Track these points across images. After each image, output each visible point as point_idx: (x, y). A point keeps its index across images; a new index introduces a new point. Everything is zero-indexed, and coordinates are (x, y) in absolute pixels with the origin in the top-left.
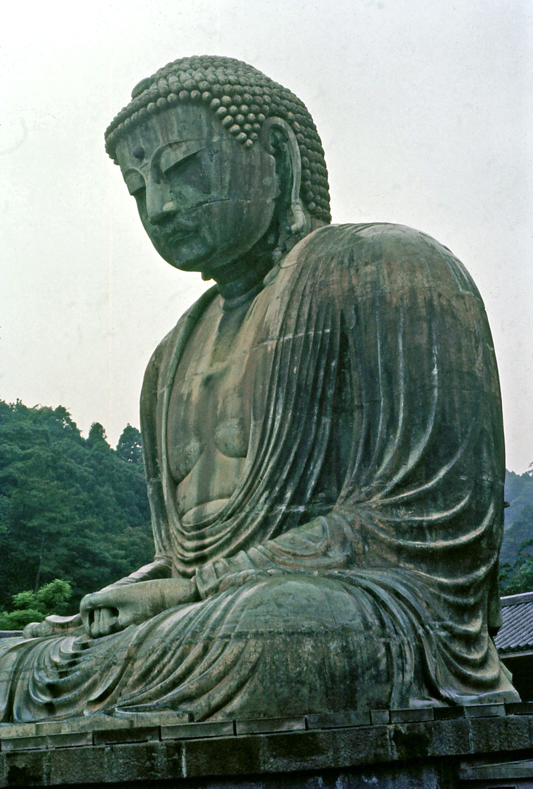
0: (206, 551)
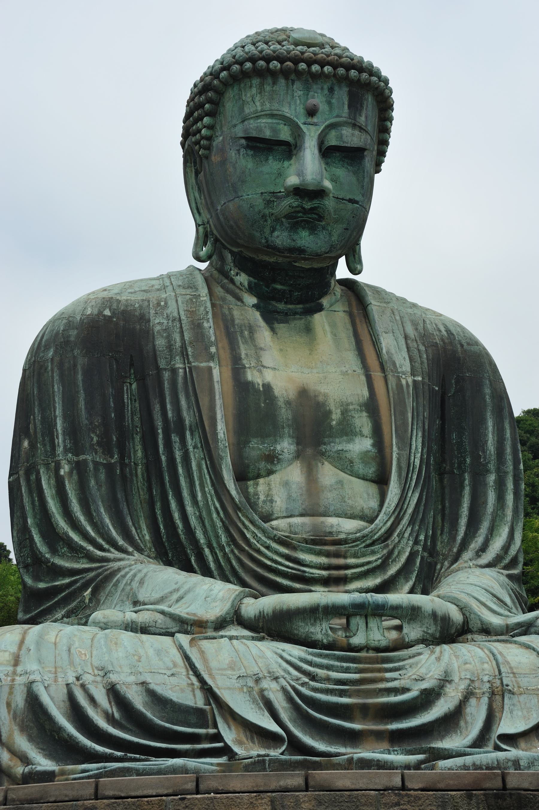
0: (349, 572)
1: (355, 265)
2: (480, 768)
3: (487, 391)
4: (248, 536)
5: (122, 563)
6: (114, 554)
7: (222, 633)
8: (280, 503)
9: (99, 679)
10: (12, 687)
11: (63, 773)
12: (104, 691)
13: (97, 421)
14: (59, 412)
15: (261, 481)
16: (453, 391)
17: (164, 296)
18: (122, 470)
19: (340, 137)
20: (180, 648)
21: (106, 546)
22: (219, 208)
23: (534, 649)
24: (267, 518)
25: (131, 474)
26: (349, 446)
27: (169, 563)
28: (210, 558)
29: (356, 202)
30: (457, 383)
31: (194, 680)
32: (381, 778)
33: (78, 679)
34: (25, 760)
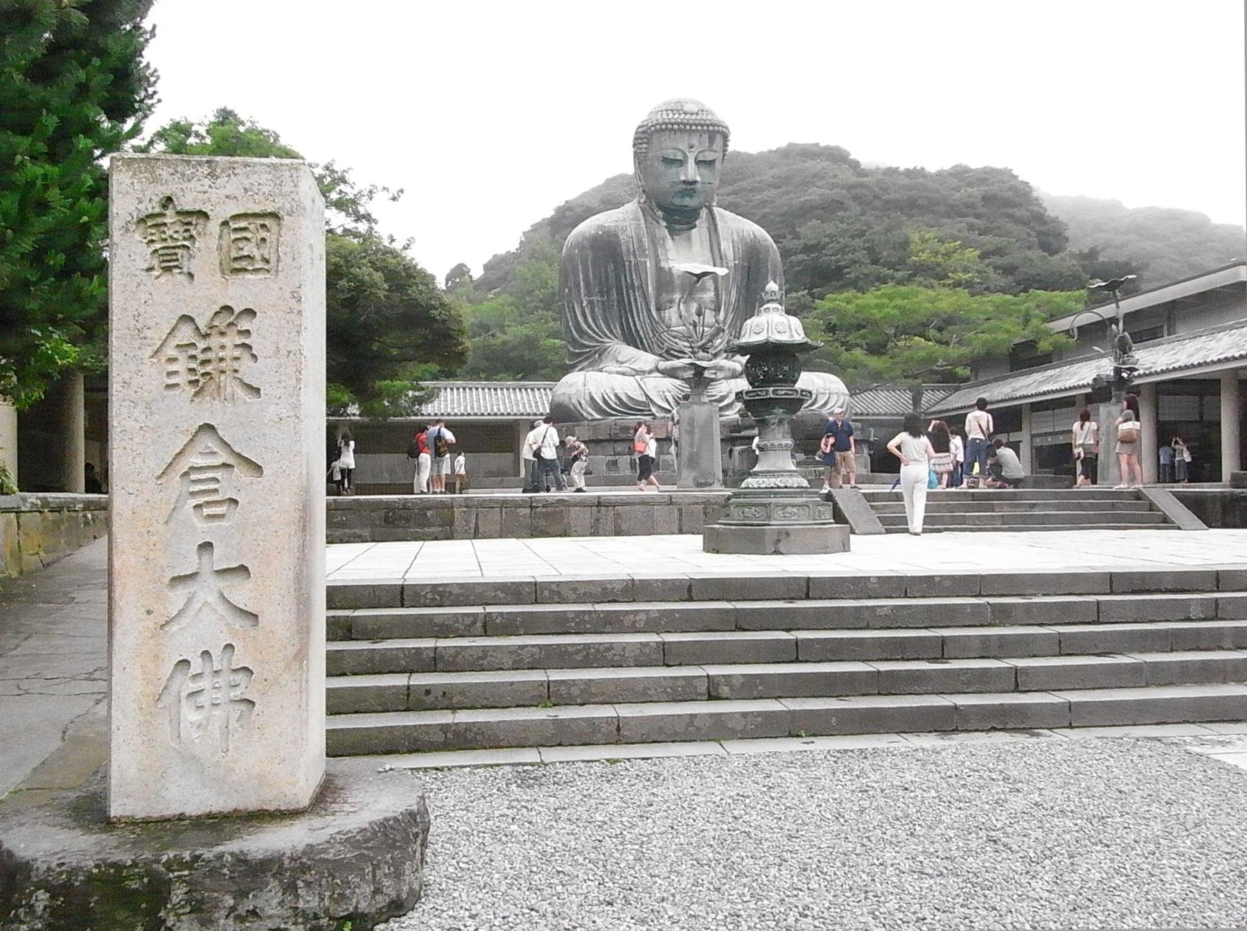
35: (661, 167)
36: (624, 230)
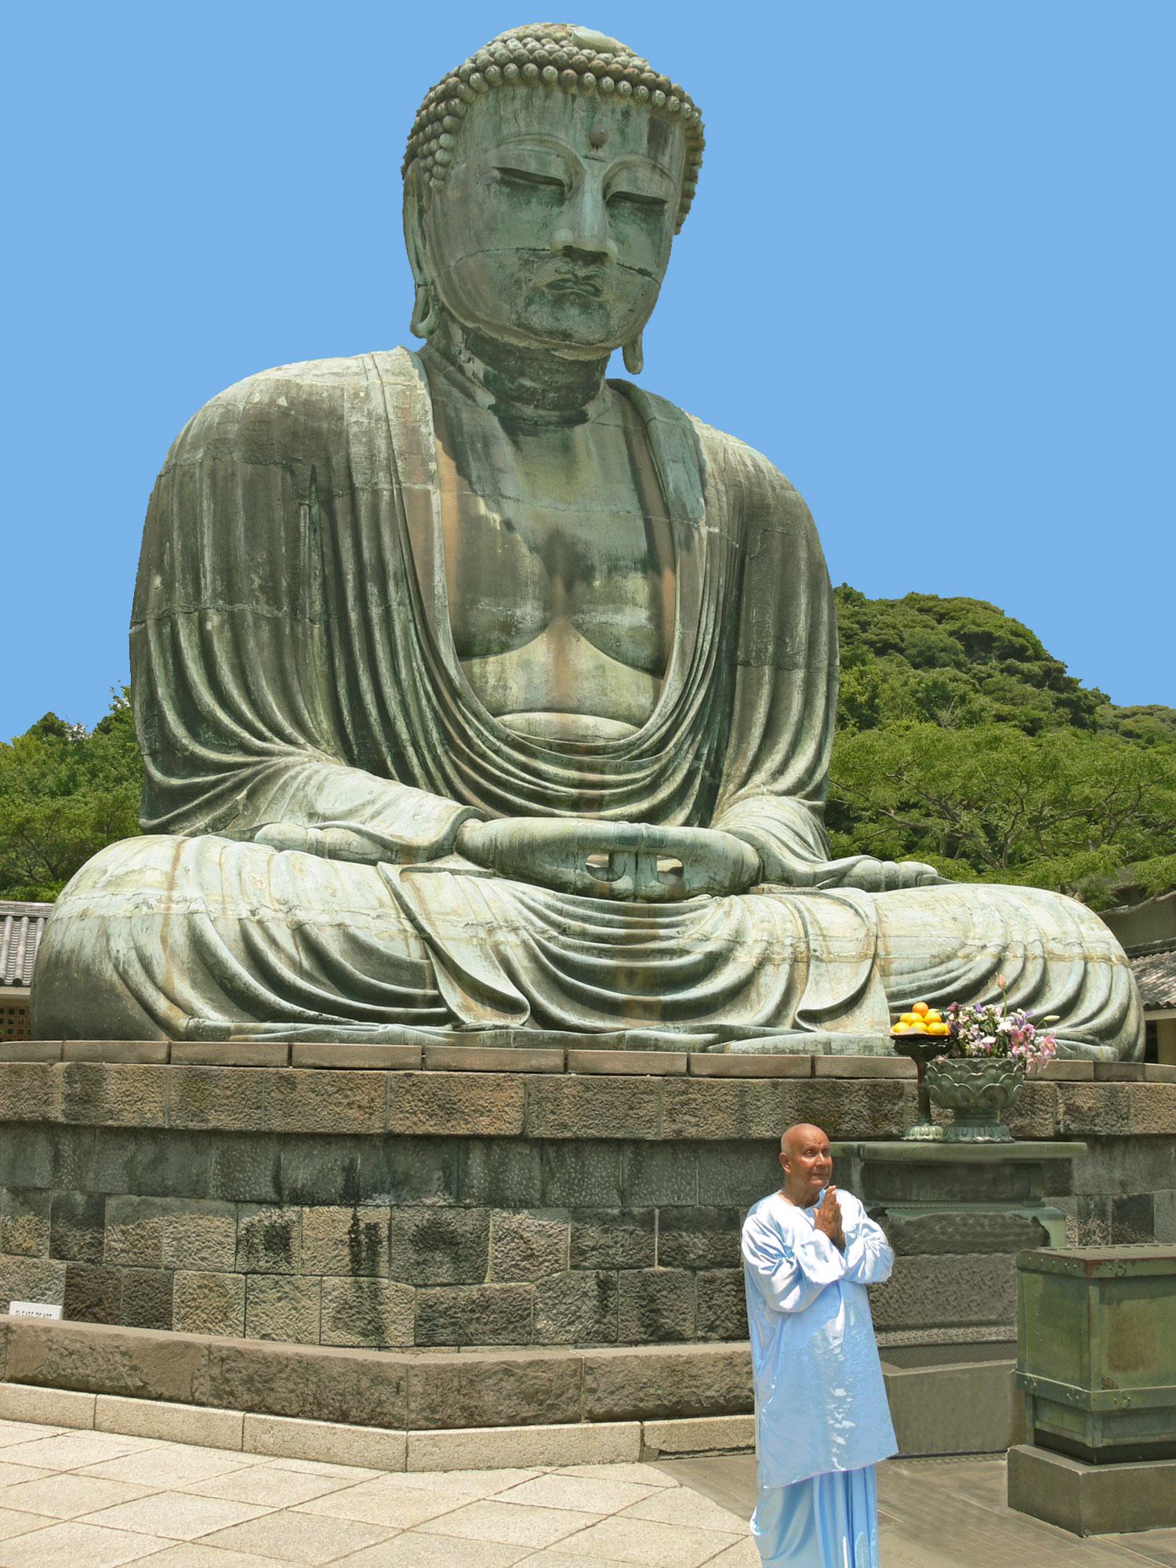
1: (633, 359)
2: (783, 1052)
3: (803, 554)
4: (471, 733)
5: (290, 759)
6: (279, 745)
7: (437, 864)
8: (516, 692)
9: (281, 915)
10: (167, 918)
11: (240, 1031)
12: (288, 932)
13: (261, 556)
14: (207, 540)
15: (491, 659)
16: (757, 550)
17: (364, 383)
18: (292, 629)
19: (634, 181)
20: (388, 882)
21: (268, 734)
22: (453, 263)
23: (851, 906)
24: (498, 712)
25: (305, 634)
26: (618, 618)
27: (352, 762)
28: (415, 761)
29: (649, 274)
30: (764, 540)
31: (408, 925)
32: (660, 1062)
33: (253, 913)
34: (190, 1012)
35: (497, 202)
36: (361, 398)
